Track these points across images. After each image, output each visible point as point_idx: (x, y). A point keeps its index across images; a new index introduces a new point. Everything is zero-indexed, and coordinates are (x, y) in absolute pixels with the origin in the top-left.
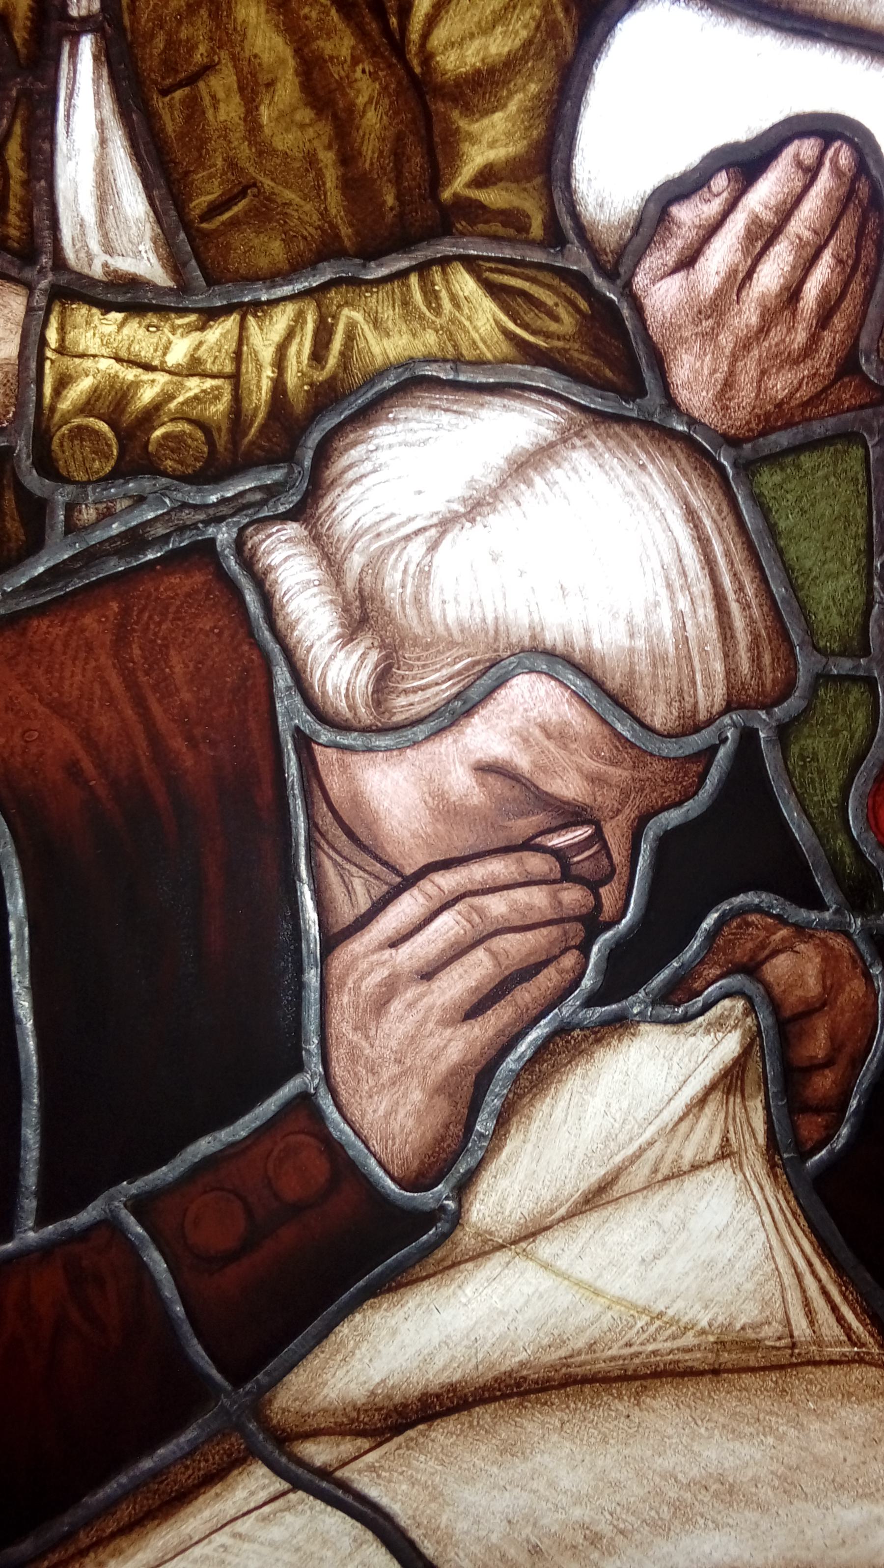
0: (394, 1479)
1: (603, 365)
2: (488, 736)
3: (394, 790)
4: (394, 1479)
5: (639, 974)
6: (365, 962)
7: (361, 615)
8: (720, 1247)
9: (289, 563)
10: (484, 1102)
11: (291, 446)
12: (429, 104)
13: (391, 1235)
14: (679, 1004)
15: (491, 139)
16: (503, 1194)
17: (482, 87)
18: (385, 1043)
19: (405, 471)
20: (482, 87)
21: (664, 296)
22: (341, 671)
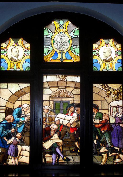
0: (52, 140)
1: (55, 124)
2: (53, 129)
3: (52, 130)
4: (52, 140)
5: (56, 133)
6: (51, 133)
7: (51, 127)
8: (57, 137)
9: (50, 126)
10: (53, 135)
11: (50, 125)
12: (53, 119)
13: (52, 137)
14: (56, 133)
15: (54, 120)
16: (53, 136)
17: (53, 119)
18: (52, 134)
19: (52, 125)
20: (53, 119)
21: (56, 122)
22: (51, 128)
